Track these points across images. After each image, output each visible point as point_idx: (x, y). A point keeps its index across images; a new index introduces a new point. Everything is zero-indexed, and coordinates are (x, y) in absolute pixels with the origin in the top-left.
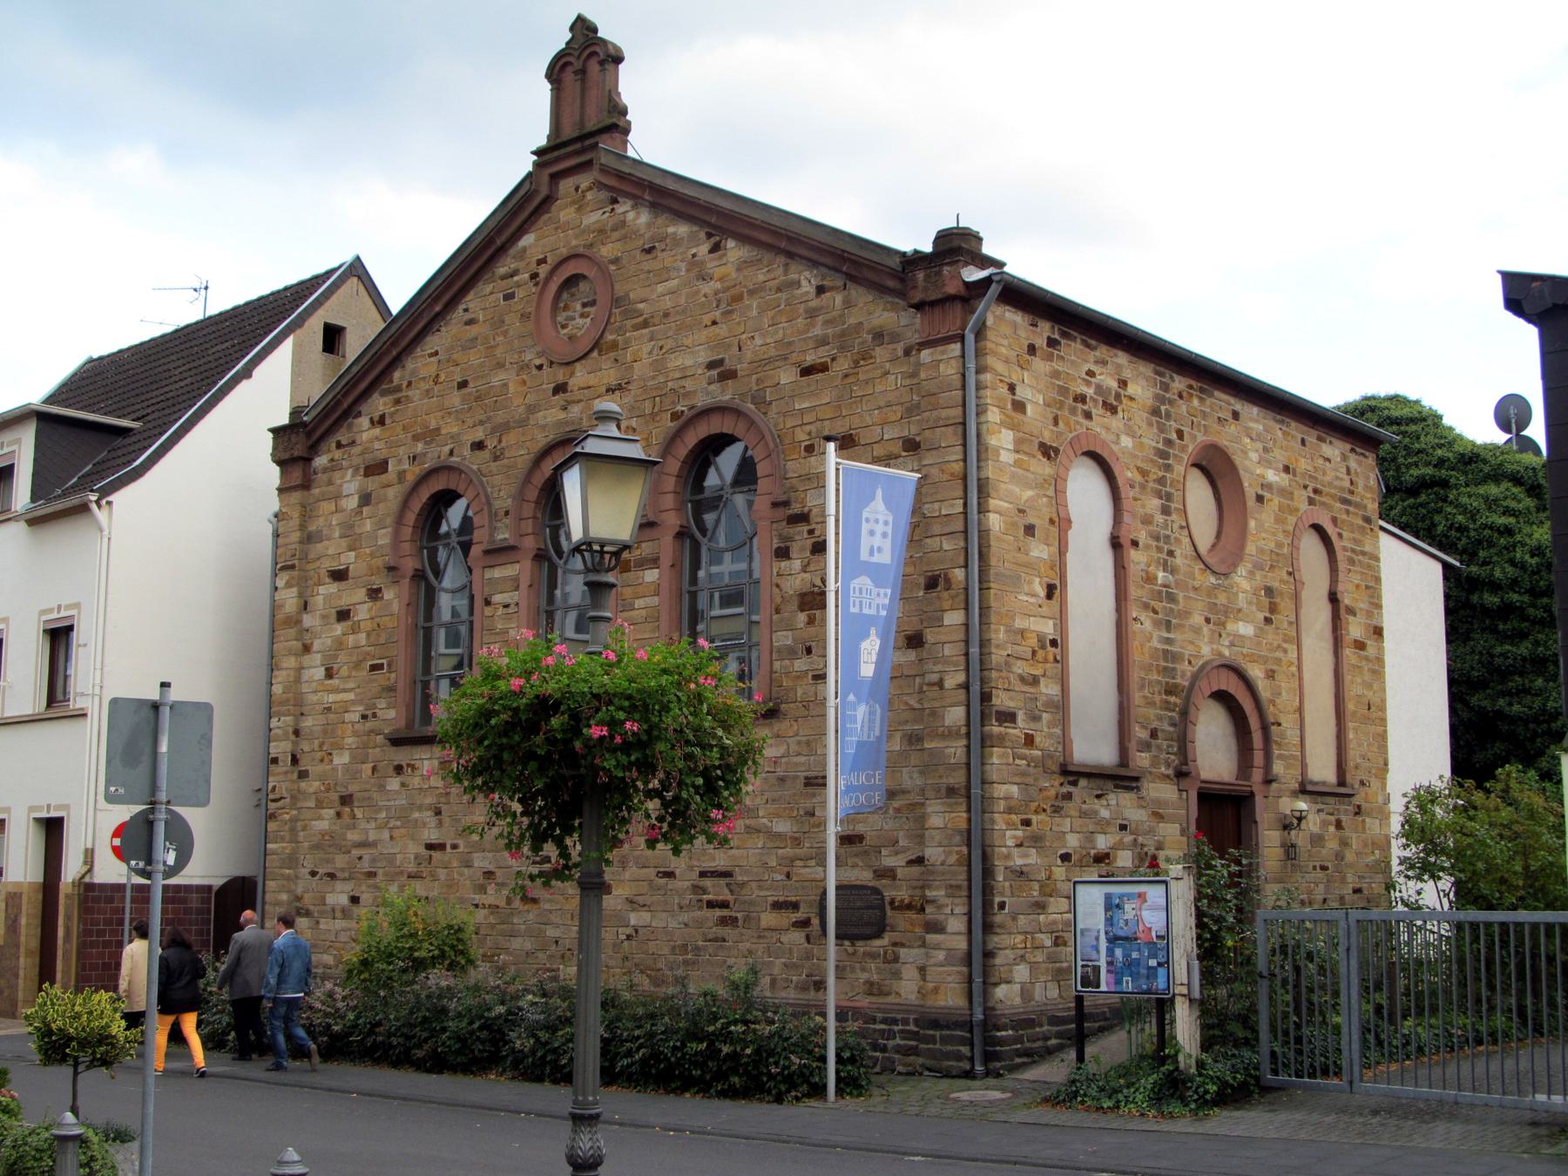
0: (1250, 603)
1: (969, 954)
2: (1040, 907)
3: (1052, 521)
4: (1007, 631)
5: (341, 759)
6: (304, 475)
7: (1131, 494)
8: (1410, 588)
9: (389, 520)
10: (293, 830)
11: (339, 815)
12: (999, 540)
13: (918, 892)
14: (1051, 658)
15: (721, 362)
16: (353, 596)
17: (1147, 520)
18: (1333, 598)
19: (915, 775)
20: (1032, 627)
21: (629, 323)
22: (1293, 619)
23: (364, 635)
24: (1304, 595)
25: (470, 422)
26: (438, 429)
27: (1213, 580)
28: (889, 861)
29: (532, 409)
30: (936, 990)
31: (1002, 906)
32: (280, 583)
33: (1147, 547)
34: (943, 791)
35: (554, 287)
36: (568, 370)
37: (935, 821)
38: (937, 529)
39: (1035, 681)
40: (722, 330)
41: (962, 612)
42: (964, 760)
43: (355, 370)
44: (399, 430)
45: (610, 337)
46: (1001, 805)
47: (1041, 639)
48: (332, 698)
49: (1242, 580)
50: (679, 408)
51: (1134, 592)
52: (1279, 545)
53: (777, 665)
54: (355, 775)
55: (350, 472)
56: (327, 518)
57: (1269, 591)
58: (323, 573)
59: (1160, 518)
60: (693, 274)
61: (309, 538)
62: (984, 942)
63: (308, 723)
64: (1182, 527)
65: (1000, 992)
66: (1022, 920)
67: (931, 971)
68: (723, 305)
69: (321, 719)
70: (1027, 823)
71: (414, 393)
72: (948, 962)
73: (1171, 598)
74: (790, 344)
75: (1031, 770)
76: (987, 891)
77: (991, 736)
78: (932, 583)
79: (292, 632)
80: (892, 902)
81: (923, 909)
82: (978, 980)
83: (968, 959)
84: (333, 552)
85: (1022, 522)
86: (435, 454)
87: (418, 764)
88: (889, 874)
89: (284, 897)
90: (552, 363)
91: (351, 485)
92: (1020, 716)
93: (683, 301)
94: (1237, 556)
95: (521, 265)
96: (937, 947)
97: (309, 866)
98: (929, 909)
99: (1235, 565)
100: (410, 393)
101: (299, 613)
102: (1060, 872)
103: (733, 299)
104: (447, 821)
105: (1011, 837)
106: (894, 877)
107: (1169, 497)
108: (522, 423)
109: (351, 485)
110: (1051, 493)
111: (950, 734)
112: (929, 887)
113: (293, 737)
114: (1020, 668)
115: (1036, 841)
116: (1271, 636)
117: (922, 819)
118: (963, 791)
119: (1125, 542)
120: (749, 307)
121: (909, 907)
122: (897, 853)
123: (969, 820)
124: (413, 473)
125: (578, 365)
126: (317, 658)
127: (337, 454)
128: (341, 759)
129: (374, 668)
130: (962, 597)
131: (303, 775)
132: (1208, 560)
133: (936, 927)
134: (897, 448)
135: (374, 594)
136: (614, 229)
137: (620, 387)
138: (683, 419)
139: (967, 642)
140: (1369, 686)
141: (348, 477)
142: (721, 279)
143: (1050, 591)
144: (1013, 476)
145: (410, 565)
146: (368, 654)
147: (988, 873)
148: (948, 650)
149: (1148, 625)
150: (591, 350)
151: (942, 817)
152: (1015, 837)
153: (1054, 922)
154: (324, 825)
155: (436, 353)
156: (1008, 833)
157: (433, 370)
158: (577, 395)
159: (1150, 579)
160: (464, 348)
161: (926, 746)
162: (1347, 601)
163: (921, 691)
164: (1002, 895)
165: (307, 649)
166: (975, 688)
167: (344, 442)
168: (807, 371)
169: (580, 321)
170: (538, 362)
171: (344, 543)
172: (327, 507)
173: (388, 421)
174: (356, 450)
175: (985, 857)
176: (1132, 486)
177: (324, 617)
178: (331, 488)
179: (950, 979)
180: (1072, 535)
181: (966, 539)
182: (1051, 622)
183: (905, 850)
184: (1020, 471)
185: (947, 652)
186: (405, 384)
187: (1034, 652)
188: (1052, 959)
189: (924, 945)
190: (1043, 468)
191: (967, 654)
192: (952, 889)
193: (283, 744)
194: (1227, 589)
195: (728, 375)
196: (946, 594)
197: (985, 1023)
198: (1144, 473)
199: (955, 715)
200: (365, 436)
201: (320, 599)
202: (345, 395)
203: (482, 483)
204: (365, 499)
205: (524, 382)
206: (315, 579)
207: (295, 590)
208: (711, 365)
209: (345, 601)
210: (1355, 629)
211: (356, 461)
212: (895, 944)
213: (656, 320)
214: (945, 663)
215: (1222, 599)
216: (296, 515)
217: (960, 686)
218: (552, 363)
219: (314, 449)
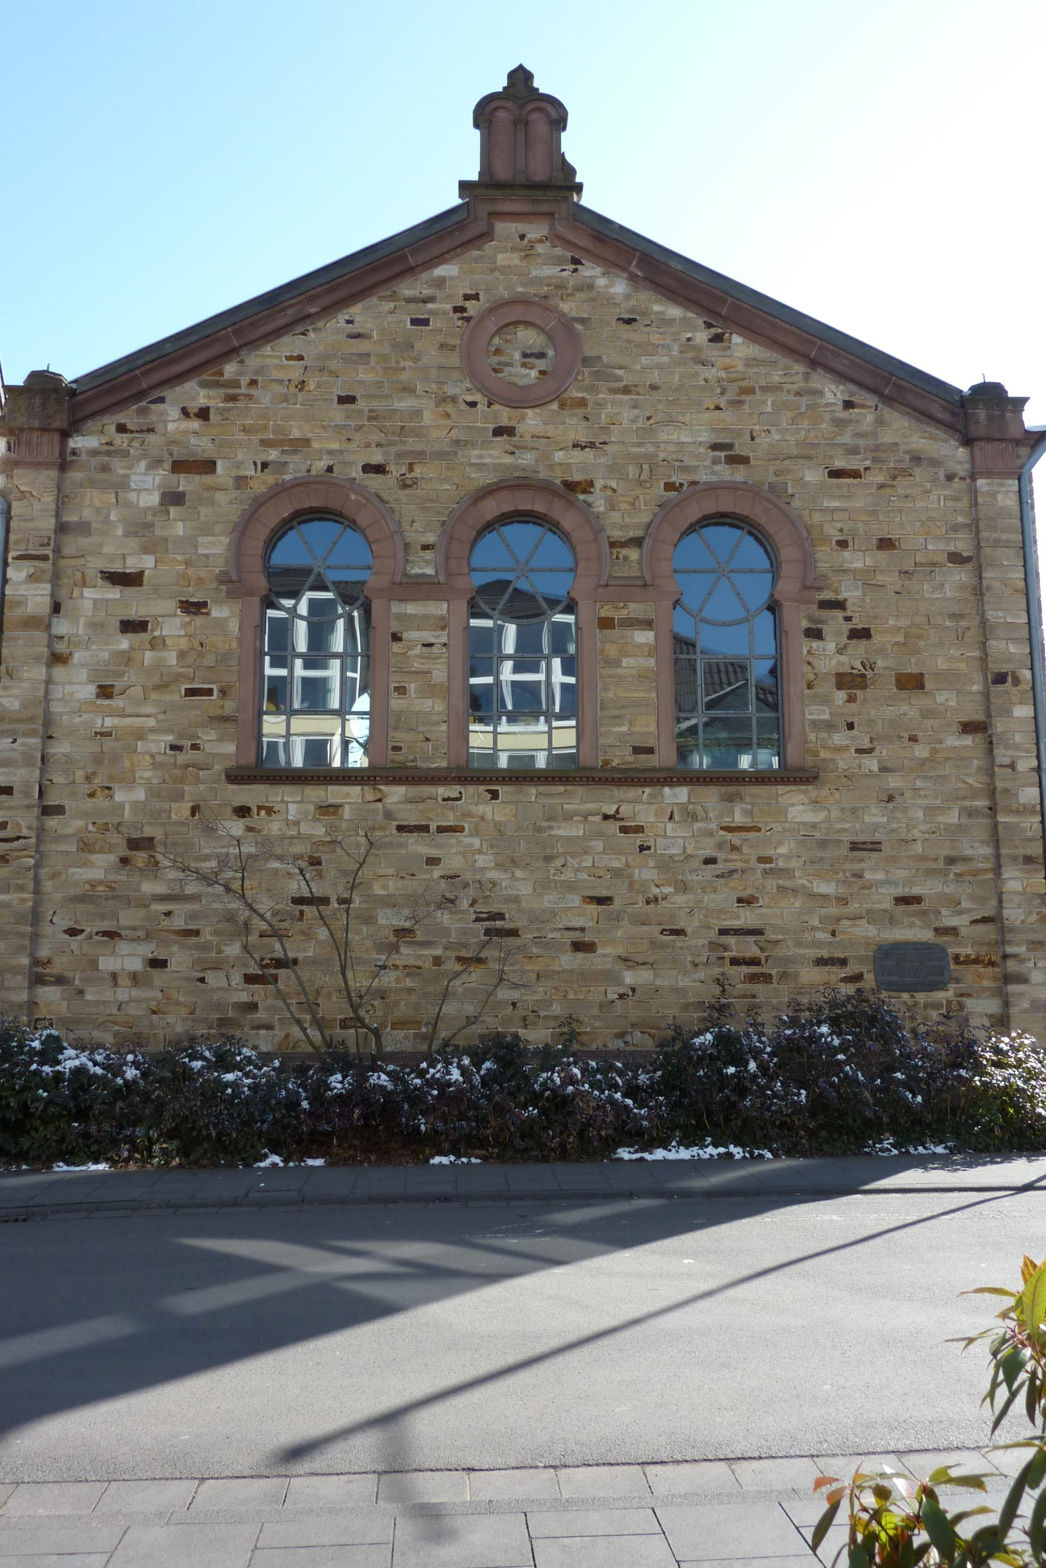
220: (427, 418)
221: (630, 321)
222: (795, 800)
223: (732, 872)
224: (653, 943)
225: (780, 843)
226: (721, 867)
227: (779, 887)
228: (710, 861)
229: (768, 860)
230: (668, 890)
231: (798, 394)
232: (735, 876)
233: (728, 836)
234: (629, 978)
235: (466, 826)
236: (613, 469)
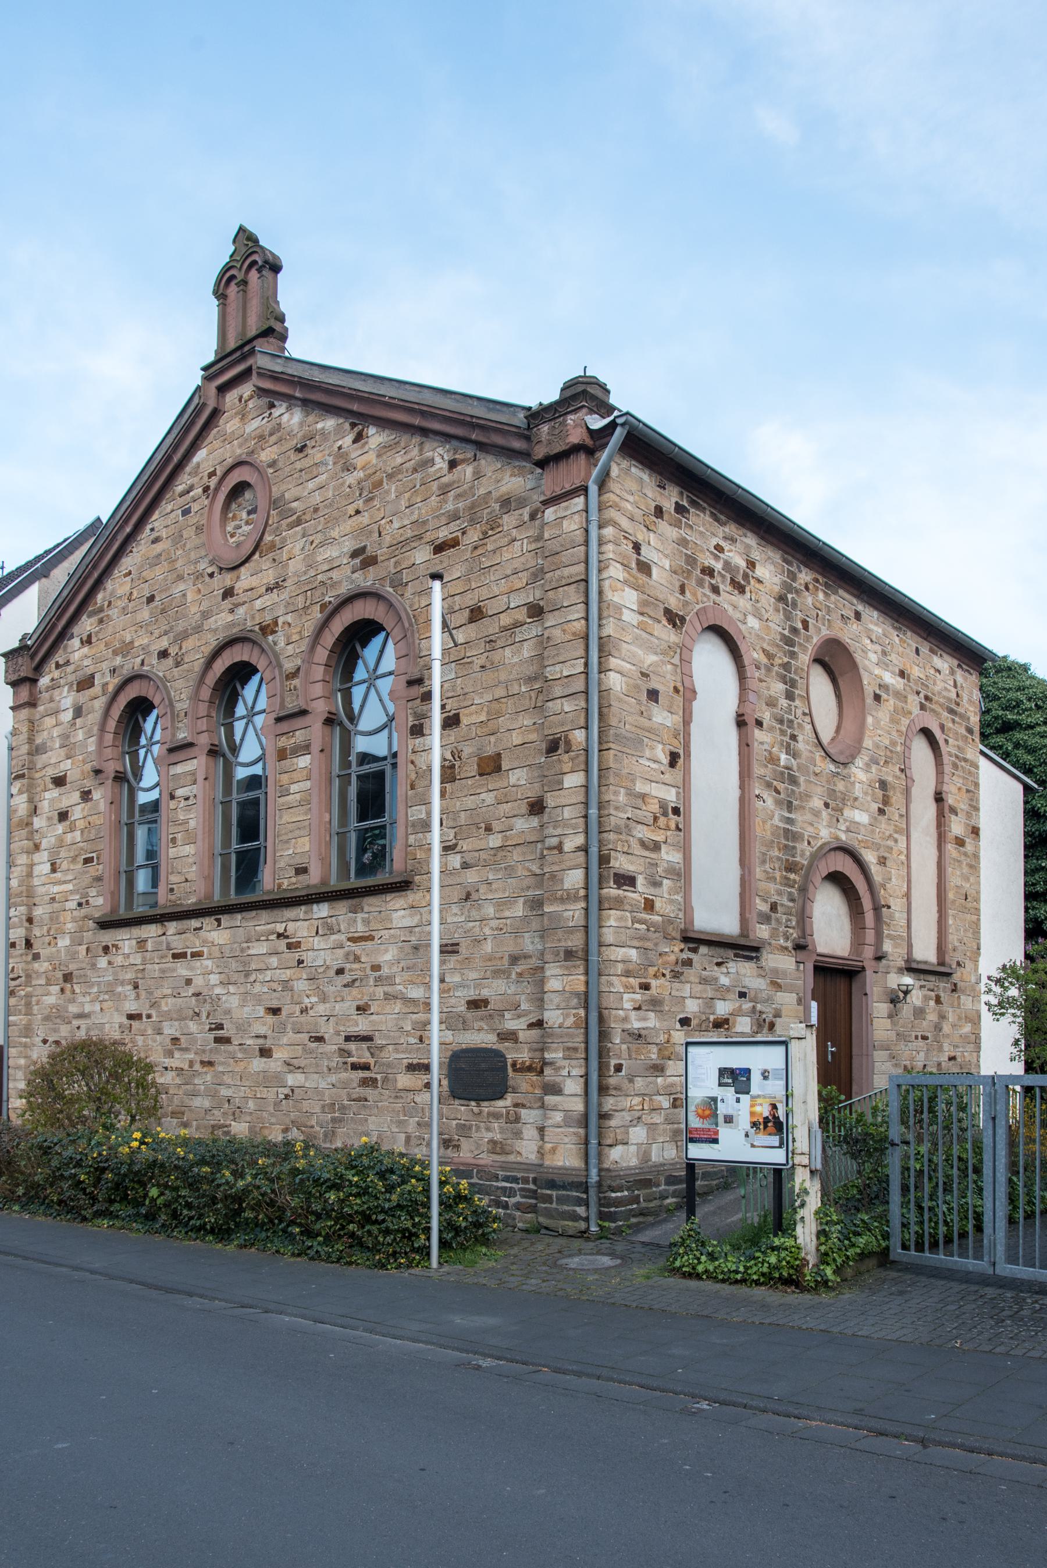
0: (866, 794)
1: (586, 1116)
2: (658, 1069)
3: (676, 690)
4: (627, 794)
5: (64, 942)
6: (31, 694)
7: (757, 674)
8: (998, 796)
9: (96, 728)
10: (28, 1005)
11: (62, 990)
12: (620, 700)
13: (538, 1054)
14: (673, 826)
15: (363, 550)
16: (70, 798)
17: (771, 703)
18: (939, 798)
19: (537, 940)
20: (654, 793)
21: (284, 523)
22: (903, 811)
23: (79, 833)
24: (915, 791)
25: (156, 633)
26: (132, 642)
27: (832, 767)
28: (511, 1024)
29: (206, 615)
30: (553, 1150)
31: (618, 1068)
32: (14, 790)
33: (771, 729)
34: (562, 954)
35: (222, 497)
36: (235, 573)
37: (553, 984)
38: (558, 691)
39: (656, 847)
40: (364, 519)
41: (582, 774)
42: (583, 923)
43: (65, 593)
44: (102, 646)
45: (268, 538)
46: (620, 968)
47: (663, 805)
48: (56, 889)
49: (860, 773)
50: (327, 599)
51: (758, 770)
52: (894, 743)
53: (412, 839)
54: (73, 956)
55: (66, 688)
56: (50, 731)
57: (883, 785)
58: (48, 780)
59: (784, 702)
60: (339, 467)
61: (36, 750)
62: (600, 1105)
63: (38, 912)
64: (804, 714)
65: (615, 1154)
66: (639, 1082)
67: (549, 1132)
68: (365, 493)
69: (48, 908)
70: (646, 987)
71: (114, 612)
72: (567, 1123)
73: (793, 780)
74: (425, 523)
75: (651, 935)
76: (603, 1053)
77: (609, 899)
78: (553, 747)
79: (24, 833)
80: (514, 1065)
81: (542, 1071)
82: (594, 1141)
83: (584, 1121)
84: (55, 761)
85: (644, 687)
86: (131, 664)
87: (120, 944)
88: (509, 1036)
89: (22, 1061)
90: (221, 569)
91: (67, 699)
92: (640, 881)
93: (330, 494)
94: (856, 749)
95: (196, 480)
96: (555, 1109)
97: (42, 1036)
98: (548, 1071)
99: (853, 757)
100: (110, 613)
101: (30, 816)
102: (679, 1036)
103: (371, 488)
104: (143, 994)
105: (628, 1001)
106: (516, 1040)
107: (793, 684)
108: (198, 629)
109: (67, 699)
110: (676, 660)
111: (569, 897)
113: (27, 925)
114: (642, 832)
115: (655, 1004)
116: (884, 826)
117: (542, 982)
118: (580, 954)
119: (751, 722)
120: (388, 492)
121: (530, 1069)
122: (519, 1017)
123: (587, 983)
124: (113, 683)
125: (243, 569)
126: (43, 856)
127: (56, 674)
128: (64, 942)
129: (87, 861)
130: (582, 758)
131: (36, 957)
132: (832, 751)
133: (555, 1089)
134: (521, 615)
135: (86, 796)
136: (271, 435)
137: (277, 586)
138: (330, 608)
139: (586, 804)
140: (967, 879)
141: (65, 694)
142: (363, 468)
143: (674, 759)
144: (637, 638)
145: (111, 768)
146: (82, 849)
147: (604, 1035)
148: (567, 813)
149: (770, 802)
150: (253, 553)
151: (562, 981)
152: (633, 1000)
153: (672, 1085)
154: (51, 1000)
155: (130, 573)
156: (626, 996)
157: (127, 588)
158: (242, 598)
159: (773, 760)
160: (153, 565)
161: (546, 910)
162: (950, 800)
163: (543, 857)
164: (620, 1058)
165: (37, 847)
166: (594, 850)
167: (61, 663)
168: (439, 549)
169: (246, 529)
170: (210, 570)
171: (62, 752)
172: (49, 721)
173: (94, 640)
174: (70, 669)
175: (601, 1019)
176: (758, 668)
177: (49, 819)
178: (52, 705)
179: (566, 1140)
180: (696, 705)
181: (587, 700)
182: (673, 791)
183: (526, 1013)
184: (644, 635)
185: (566, 815)
186: (106, 603)
187: (656, 819)
188: (668, 1121)
189: (543, 1106)
190: (665, 633)
191: (586, 817)
193: (19, 930)
194: (845, 778)
195: (370, 562)
196: (565, 757)
197: (599, 1184)
198: (769, 656)
199: (574, 879)
200: (77, 656)
201: (46, 803)
202: (59, 619)
203: (166, 687)
204: (78, 712)
205: (199, 590)
206: (42, 787)
207: (25, 795)
208: (355, 554)
209: (64, 804)
210: (957, 827)
211: (71, 678)
212: (516, 1105)
213: (307, 517)
214: (565, 826)
215: (840, 786)
216: (25, 729)
217: (579, 849)
218: (221, 569)
219: (38, 668)
223: (354, 981)
225: (386, 951)
226: (347, 978)
227: (385, 994)
228: (340, 972)
230: (314, 999)
232: (357, 984)
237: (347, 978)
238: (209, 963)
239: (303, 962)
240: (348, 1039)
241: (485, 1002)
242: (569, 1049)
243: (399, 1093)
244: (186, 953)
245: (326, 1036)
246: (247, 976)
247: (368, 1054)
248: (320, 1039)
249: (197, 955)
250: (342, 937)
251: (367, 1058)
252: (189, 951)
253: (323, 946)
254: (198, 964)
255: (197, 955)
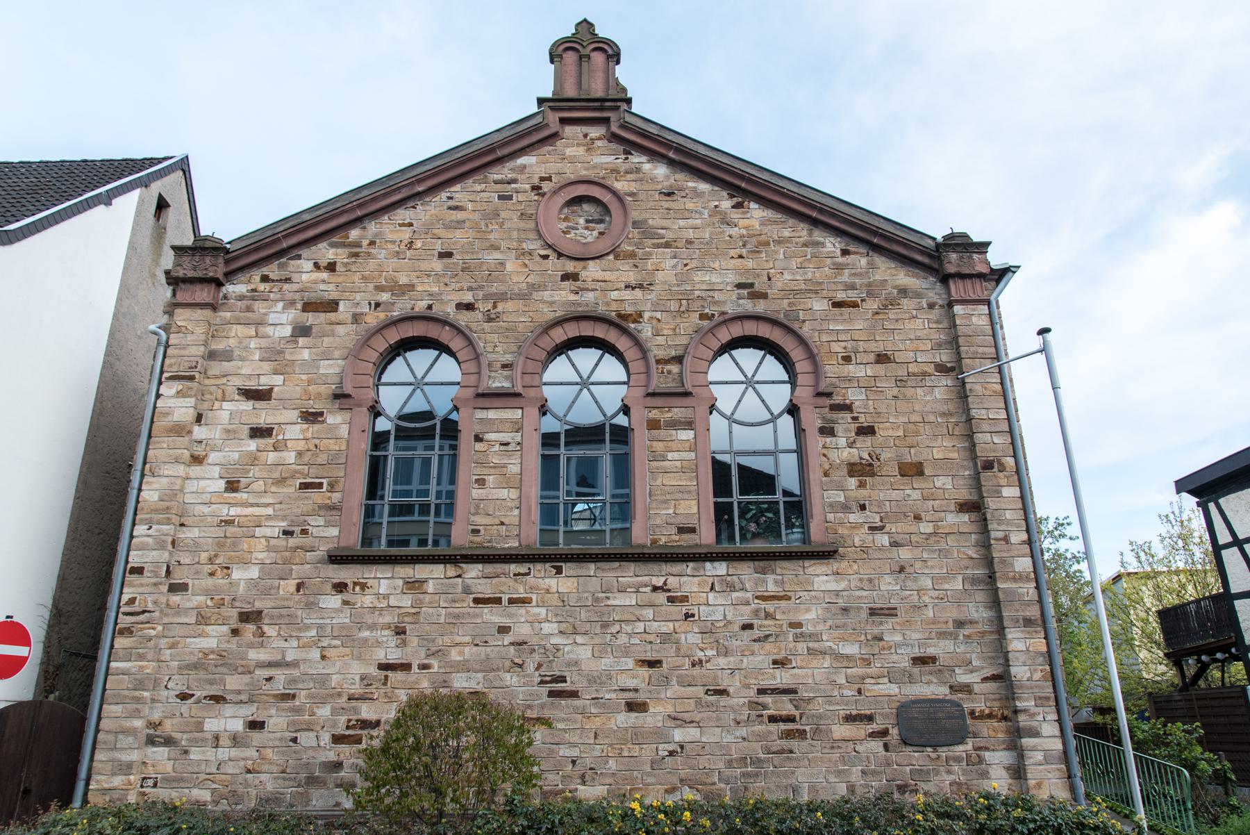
28: (964, 678)
112: (1019, 699)
192: (1040, 701)
220: (509, 267)
221: (669, 194)
222: (819, 571)
223: (767, 637)
224: (698, 701)
225: (808, 610)
226: (756, 633)
228: (747, 627)
229: (800, 625)
230: (710, 653)
231: (805, 245)
232: (771, 639)
233: (763, 605)
234: (678, 735)
235: (534, 597)
236: (656, 306)
237: (756, 633)
238: (543, 611)
239: (693, 615)
240: (761, 691)
241: (933, 659)
242: (1040, 698)
243: (835, 744)
244: (500, 598)
245: (731, 690)
246: (605, 625)
247: (791, 707)
248: (722, 692)
249: (524, 601)
250: (749, 595)
251: (787, 708)
252: (505, 598)
253: (720, 601)
254: (523, 611)
255: (524, 601)
